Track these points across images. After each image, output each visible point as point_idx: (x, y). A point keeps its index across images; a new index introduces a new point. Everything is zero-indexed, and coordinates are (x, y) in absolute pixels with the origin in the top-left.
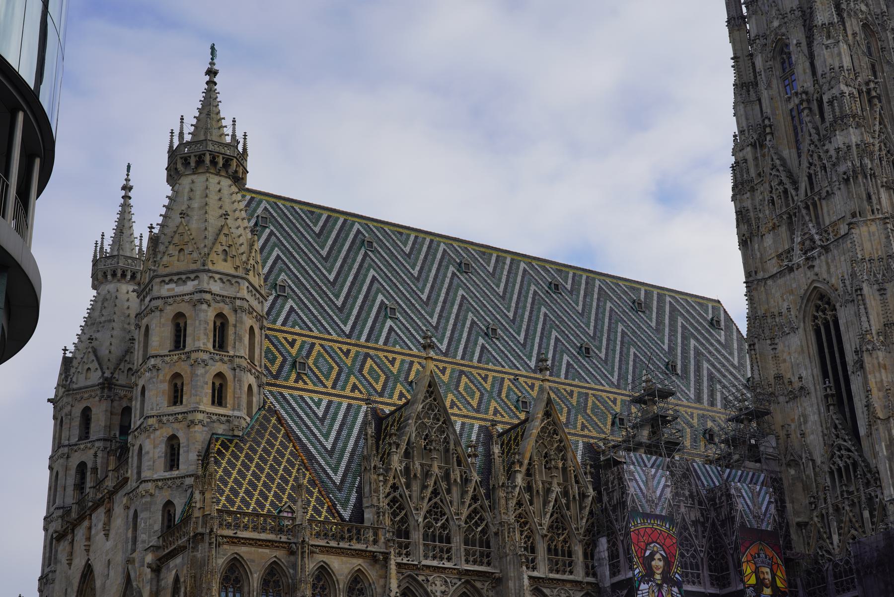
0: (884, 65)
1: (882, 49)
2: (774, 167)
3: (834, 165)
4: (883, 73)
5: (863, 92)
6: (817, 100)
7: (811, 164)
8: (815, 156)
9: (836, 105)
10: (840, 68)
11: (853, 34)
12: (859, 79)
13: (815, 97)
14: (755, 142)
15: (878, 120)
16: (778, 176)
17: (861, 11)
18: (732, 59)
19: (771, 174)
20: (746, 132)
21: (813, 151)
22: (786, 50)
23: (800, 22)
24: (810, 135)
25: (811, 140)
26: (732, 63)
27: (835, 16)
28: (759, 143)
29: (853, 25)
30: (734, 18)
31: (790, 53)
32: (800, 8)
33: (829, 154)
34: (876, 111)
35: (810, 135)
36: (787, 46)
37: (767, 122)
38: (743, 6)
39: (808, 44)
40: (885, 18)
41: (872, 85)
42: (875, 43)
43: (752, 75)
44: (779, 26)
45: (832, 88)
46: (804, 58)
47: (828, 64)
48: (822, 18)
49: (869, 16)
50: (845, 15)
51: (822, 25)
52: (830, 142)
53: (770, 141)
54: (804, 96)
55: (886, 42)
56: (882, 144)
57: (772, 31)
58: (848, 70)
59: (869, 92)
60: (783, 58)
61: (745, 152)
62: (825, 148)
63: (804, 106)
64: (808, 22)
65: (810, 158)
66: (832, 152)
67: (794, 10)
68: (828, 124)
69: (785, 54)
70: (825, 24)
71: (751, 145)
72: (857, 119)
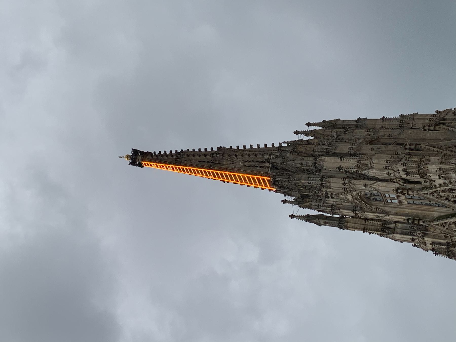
1: (389, 137)
2: (443, 225)
3: (451, 183)
4: (405, 139)
5: (409, 153)
6: (404, 183)
7: (447, 199)
8: (442, 194)
9: (410, 170)
11: (372, 150)
13: (402, 184)
14: (422, 233)
15: (431, 148)
16: (450, 224)
18: (364, 232)
19: (447, 229)
20: (414, 237)
21: (438, 195)
22: (368, 196)
23: (353, 181)
24: (427, 194)
25: (430, 194)
26: (367, 234)
28: (424, 231)
29: (366, 149)
30: (340, 223)
31: (371, 194)
32: (344, 179)
33: (442, 184)
34: (425, 148)
35: (427, 194)
38: (335, 216)
39: (368, 180)
43: (378, 223)
44: (352, 195)
45: (399, 170)
46: (376, 184)
52: (434, 181)
53: (424, 222)
54: (399, 191)
56: (448, 149)
57: (354, 201)
58: (391, 158)
60: (373, 199)
61: (427, 242)
62: (438, 185)
63: (406, 193)
64: (354, 176)
65: (442, 199)
66: (442, 181)
67: (344, 183)
68: (422, 180)
69: (371, 197)
71: (423, 236)
72: (424, 159)
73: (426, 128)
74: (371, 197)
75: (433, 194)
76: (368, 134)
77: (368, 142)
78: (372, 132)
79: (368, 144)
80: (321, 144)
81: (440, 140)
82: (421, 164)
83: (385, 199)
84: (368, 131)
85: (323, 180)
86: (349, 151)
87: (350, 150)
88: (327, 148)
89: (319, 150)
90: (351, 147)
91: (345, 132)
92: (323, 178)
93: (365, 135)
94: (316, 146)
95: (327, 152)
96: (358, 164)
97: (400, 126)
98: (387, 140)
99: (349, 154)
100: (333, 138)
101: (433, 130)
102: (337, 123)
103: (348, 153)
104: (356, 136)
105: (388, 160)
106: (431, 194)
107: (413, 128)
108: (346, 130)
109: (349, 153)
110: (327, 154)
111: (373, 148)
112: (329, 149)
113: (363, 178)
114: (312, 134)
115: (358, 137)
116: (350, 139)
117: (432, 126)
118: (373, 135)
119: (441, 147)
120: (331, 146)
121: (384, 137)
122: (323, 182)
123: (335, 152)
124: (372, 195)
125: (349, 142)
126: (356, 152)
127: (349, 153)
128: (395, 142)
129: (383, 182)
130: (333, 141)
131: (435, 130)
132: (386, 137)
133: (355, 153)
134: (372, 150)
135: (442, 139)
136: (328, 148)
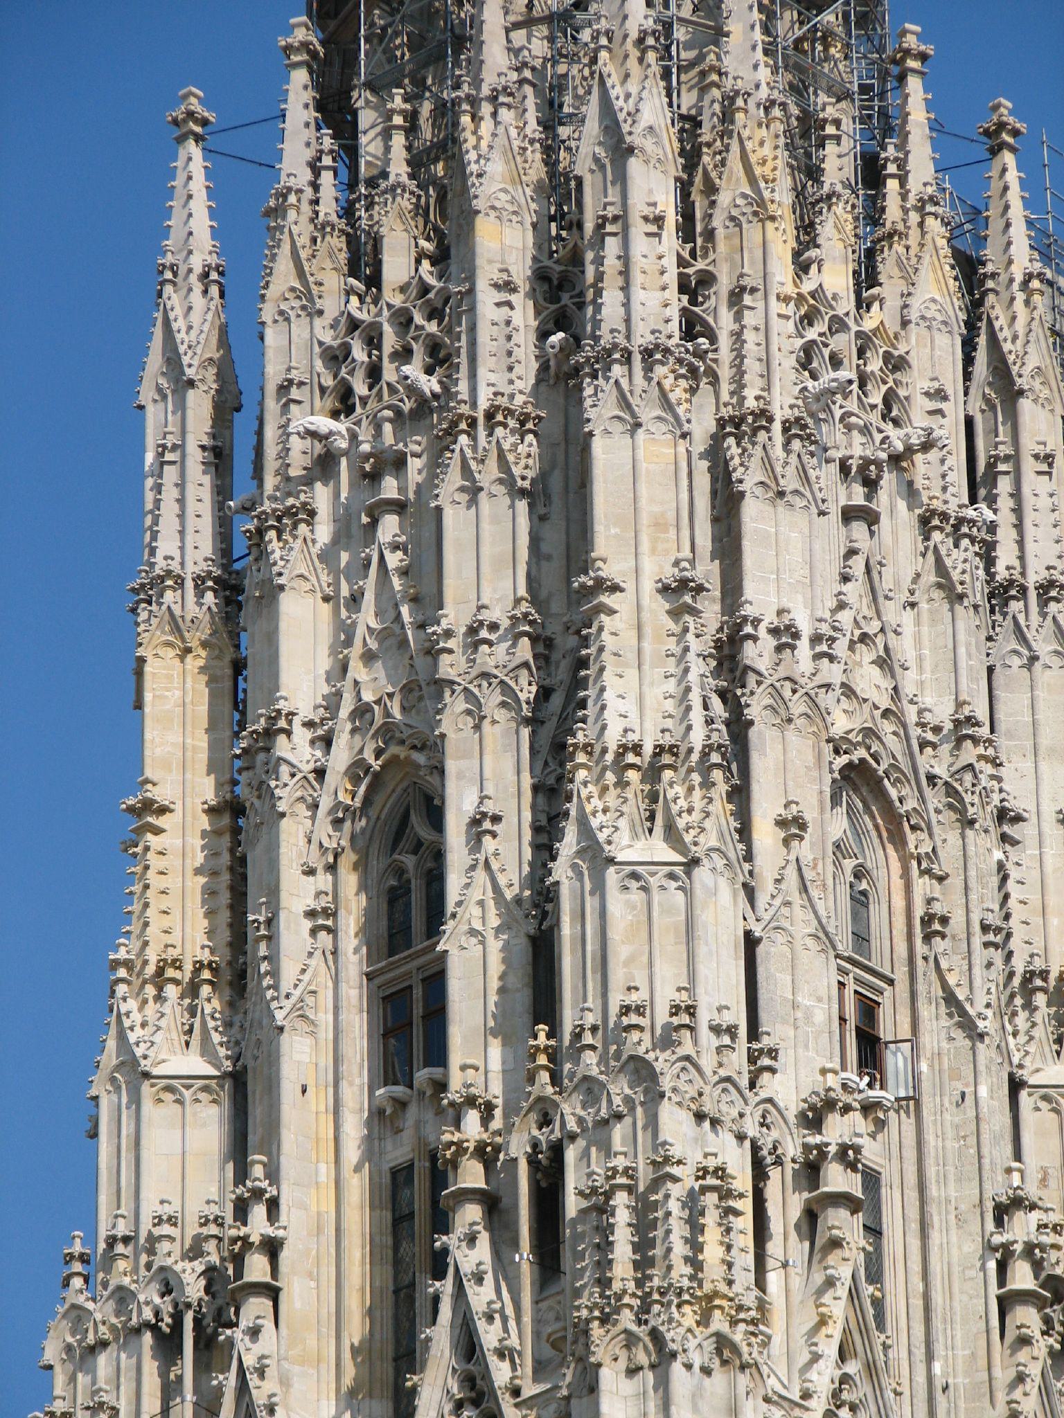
0: (926, 1012)
1: (928, 920)
5: (779, 1162)
6: (532, 1161)
9: (622, 1217)
10: (675, 1010)
11: (781, 823)
12: (770, 1085)
15: (835, 1330)
17: (848, 691)
27: (697, 716)
36: (435, 815)
37: (258, 1225)
39: (537, 829)
40: (970, 753)
41: (837, 1130)
42: (897, 883)
47: (618, 977)
48: (630, 707)
49: (887, 727)
50: (756, 707)
51: (624, 749)
55: (956, 882)
58: (716, 1030)
59: (811, 1170)
64: (557, 700)
70: (637, 749)
72: (719, 1322)
73: (1022, 1228)
74: (415, 852)
75: (476, 1403)
76: (937, 730)
77: (861, 753)
78: (953, 769)
79: (843, 760)
80: (812, 334)
81: (930, 1357)
82: (679, 1306)
83: (408, 974)
84: (957, 723)
85: (499, 431)
86: (756, 622)
87: (774, 632)
88: (771, 420)
89: (749, 336)
90: (796, 636)
91: (936, 522)
92: (512, 423)
93: (928, 700)
94: (786, 299)
95: (737, 422)
96: (648, 749)
97: (1029, 977)
98: (899, 902)
99: (739, 627)
100: (874, 418)
101: (1002, 1282)
102: (1025, 404)
103: (745, 619)
104: (918, 623)
105: (692, 1015)
106: (473, 1388)
107: (1023, 1094)
108: (956, 527)
109: (748, 629)
110: (721, 423)
111: (803, 826)
112: (762, 436)
113: (551, 781)
114: (905, 211)
115: (905, 648)
116: (886, 583)
117: (1037, 1266)
118: (932, 779)
119: (853, 1408)
120: (796, 445)
121: (923, 873)
122: (482, 433)
123: (742, 495)
124: (430, 865)
125: (854, 591)
126: (759, 683)
127: (748, 629)
128: (891, 982)
129: (530, 969)
130: (849, 428)
131: (1006, 1303)
132: (922, 886)
133: (751, 679)
134: (781, 823)
135: (937, 1367)
136: (777, 427)
